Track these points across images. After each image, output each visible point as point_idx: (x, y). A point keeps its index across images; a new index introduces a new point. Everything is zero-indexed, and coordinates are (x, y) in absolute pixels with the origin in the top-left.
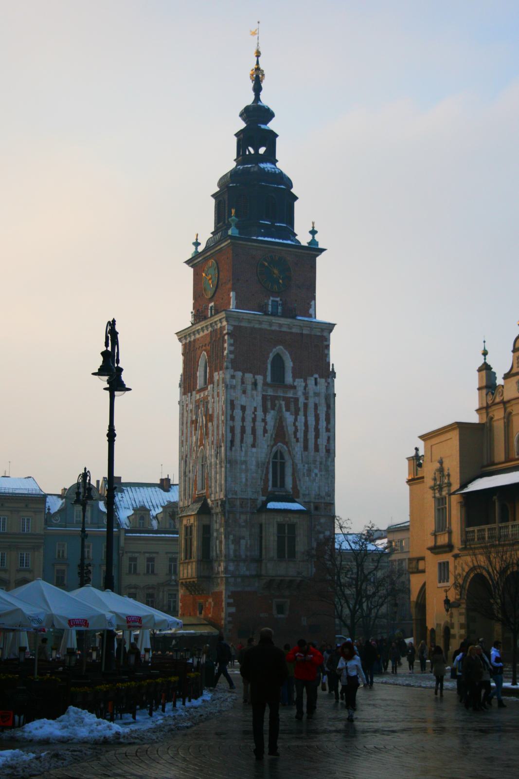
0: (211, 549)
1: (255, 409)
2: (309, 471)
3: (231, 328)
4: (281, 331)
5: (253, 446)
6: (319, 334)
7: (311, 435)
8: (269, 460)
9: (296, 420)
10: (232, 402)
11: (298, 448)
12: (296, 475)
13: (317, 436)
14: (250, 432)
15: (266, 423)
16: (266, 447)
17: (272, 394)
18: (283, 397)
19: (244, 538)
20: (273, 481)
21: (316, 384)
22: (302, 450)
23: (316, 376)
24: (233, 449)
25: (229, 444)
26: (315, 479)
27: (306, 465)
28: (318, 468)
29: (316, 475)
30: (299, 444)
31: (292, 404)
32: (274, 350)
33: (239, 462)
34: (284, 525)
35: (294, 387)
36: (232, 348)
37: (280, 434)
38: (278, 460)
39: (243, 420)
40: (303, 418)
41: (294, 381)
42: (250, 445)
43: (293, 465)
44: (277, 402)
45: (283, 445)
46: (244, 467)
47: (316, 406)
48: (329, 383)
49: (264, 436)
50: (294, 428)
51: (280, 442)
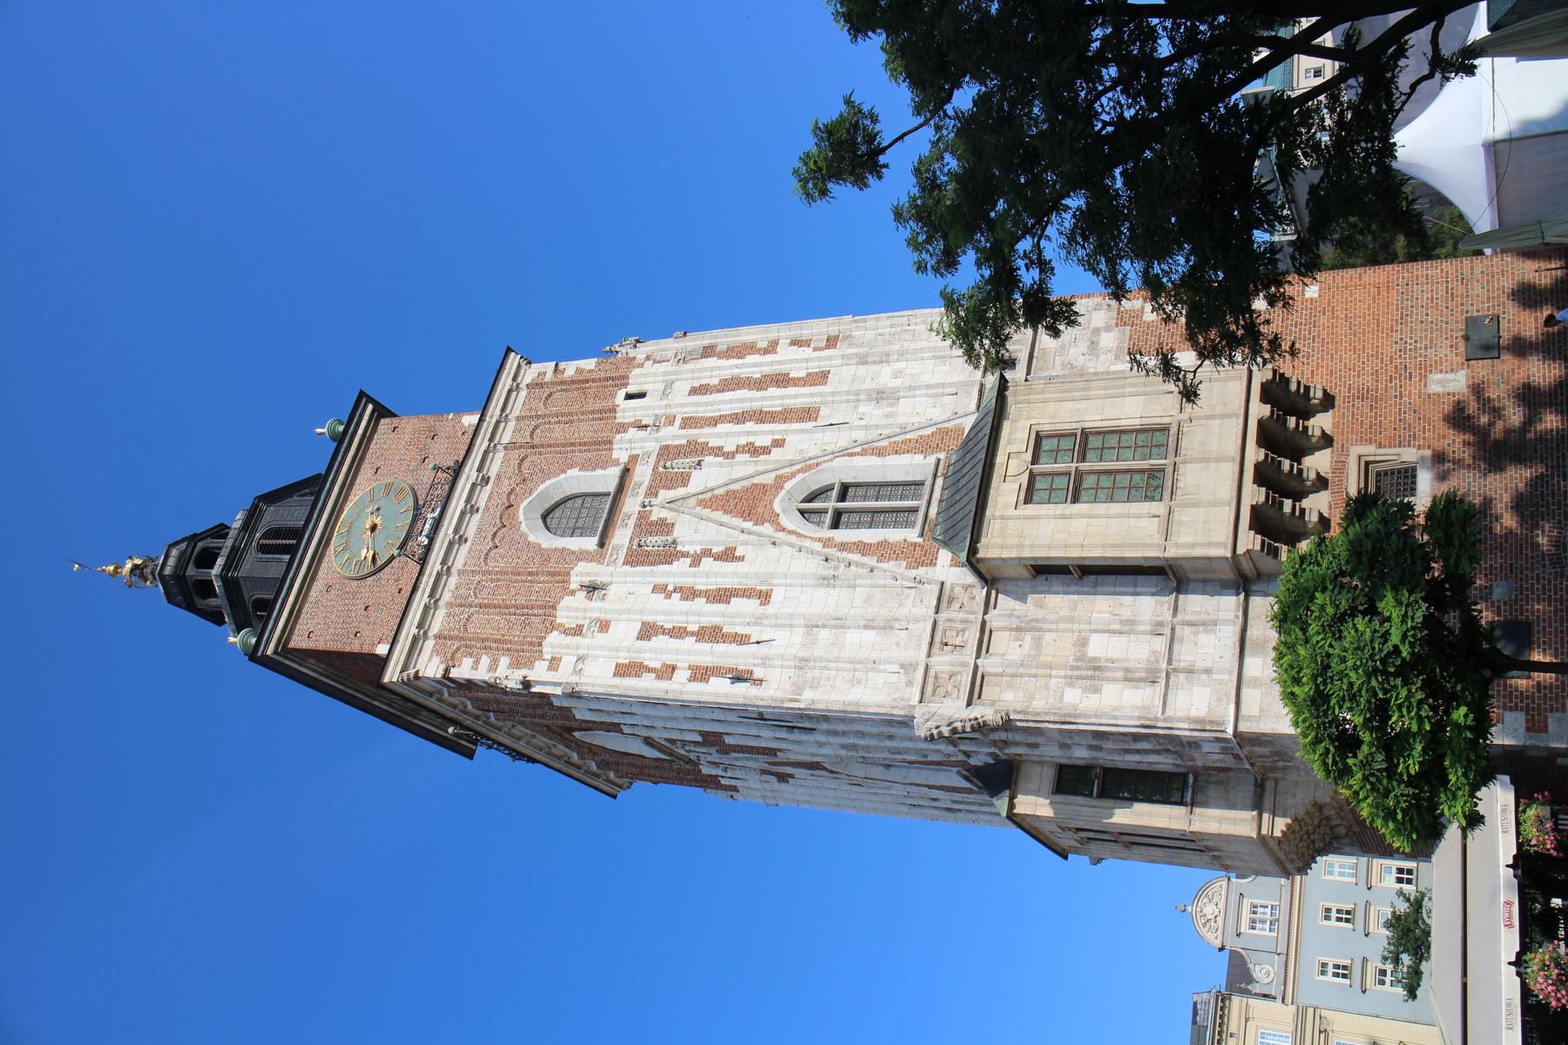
0: (1144, 767)
1: (660, 589)
2: (879, 396)
3: (436, 660)
4: (487, 508)
5: (765, 597)
6: (523, 393)
7: (774, 399)
8: (820, 540)
9: (718, 452)
10: (623, 670)
11: (801, 441)
12: (885, 443)
13: (782, 380)
14: (720, 607)
15: (707, 553)
16: (775, 551)
17: (628, 532)
18: (647, 495)
19: (1083, 643)
20: (896, 525)
21: (642, 395)
22: (810, 425)
23: (622, 393)
24: (758, 674)
25: (741, 687)
26: (913, 376)
27: (861, 409)
28: (877, 367)
29: (897, 374)
30: (789, 438)
31: (673, 465)
32: (524, 528)
33: (802, 654)
34: (1032, 477)
35: (634, 459)
36: (485, 661)
37: (747, 503)
38: (831, 504)
39: (678, 633)
40: (721, 428)
41: (617, 462)
42: (761, 609)
43: (851, 455)
44: (654, 517)
45: (782, 493)
46: (824, 635)
47: (694, 391)
48: (648, 358)
49: (741, 559)
50: (739, 457)
51: (771, 503)
